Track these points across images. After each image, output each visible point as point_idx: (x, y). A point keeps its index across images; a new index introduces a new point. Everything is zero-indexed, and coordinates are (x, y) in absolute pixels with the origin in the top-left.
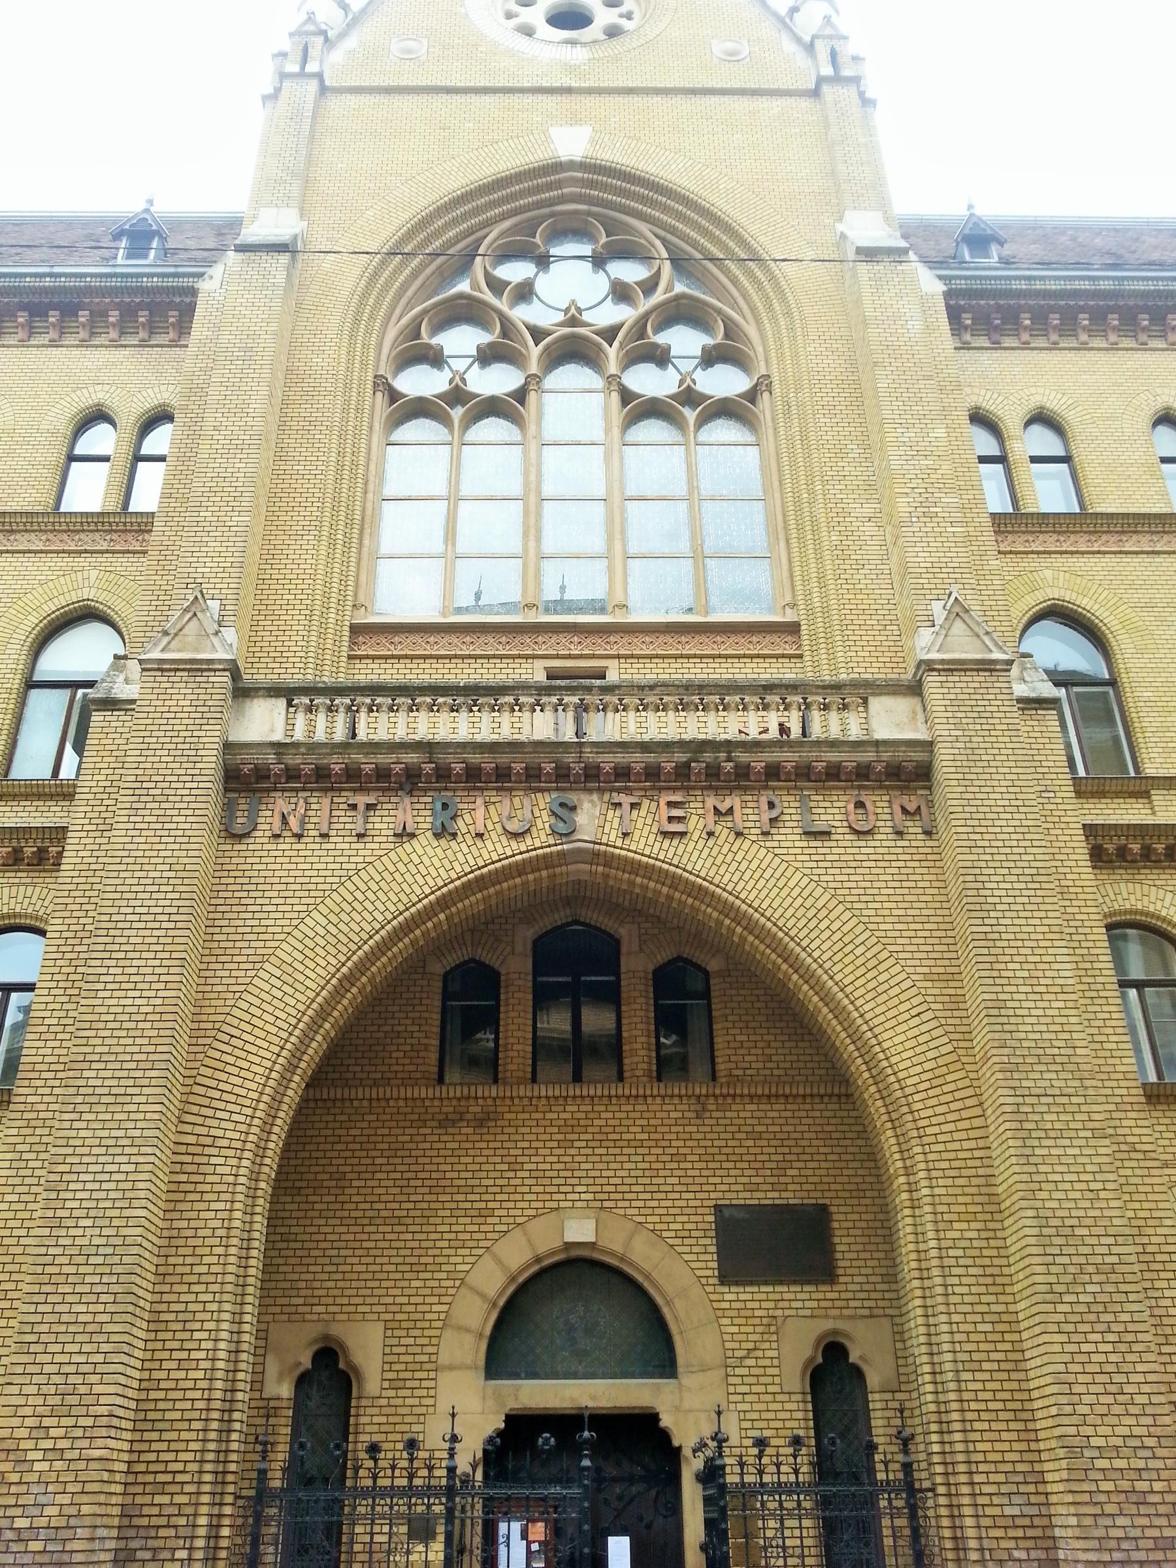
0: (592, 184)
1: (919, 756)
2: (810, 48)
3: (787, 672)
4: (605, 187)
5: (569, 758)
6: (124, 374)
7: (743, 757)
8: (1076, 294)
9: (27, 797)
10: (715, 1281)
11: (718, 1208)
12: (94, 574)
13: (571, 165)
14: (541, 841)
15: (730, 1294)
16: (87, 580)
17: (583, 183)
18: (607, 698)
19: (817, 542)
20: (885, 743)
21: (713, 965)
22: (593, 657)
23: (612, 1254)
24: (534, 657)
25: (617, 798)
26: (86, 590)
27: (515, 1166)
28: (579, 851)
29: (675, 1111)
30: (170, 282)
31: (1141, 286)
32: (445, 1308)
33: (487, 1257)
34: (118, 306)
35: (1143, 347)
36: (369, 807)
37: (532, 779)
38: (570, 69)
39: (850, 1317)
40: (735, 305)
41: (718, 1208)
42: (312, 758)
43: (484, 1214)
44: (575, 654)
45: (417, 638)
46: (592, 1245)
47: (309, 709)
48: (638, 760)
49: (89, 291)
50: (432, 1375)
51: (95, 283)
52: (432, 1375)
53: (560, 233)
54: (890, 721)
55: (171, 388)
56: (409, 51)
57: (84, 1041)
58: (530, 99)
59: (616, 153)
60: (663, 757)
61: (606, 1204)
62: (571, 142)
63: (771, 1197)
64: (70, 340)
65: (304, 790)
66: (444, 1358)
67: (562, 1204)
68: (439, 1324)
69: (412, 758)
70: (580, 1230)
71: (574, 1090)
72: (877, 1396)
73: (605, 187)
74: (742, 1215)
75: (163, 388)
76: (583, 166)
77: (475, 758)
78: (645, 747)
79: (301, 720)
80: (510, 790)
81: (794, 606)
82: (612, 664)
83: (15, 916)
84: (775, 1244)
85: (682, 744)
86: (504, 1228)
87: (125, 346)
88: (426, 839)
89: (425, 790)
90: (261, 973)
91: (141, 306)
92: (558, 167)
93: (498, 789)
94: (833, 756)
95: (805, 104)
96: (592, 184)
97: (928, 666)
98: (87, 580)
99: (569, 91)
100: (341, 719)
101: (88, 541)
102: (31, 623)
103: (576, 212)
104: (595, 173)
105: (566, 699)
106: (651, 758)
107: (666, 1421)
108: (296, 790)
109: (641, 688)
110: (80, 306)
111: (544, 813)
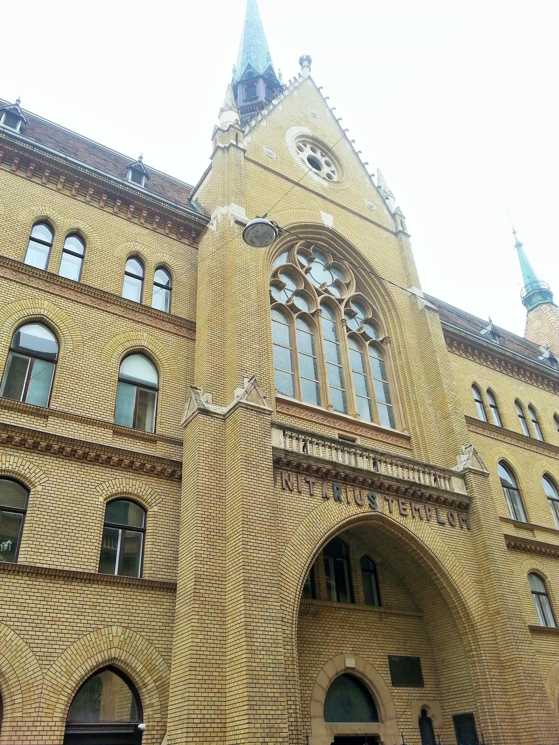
0: (332, 239)
1: (467, 501)
2: (393, 216)
3: (408, 455)
4: (336, 242)
5: (376, 479)
6: (159, 247)
7: (423, 490)
8: (455, 334)
9: (126, 435)
10: (390, 685)
11: (390, 657)
12: (145, 334)
13: (327, 229)
14: (366, 510)
15: (397, 690)
16: (145, 337)
17: (329, 237)
18: (382, 458)
19: (417, 409)
20: (458, 494)
21: (378, 560)
22: (353, 433)
23: (359, 672)
24: (335, 428)
25: (387, 497)
26: (143, 341)
27: (327, 635)
28: (377, 515)
29: (374, 617)
30: (172, 209)
31: (471, 338)
32: (310, 692)
33: (322, 672)
34: (148, 210)
35: (474, 361)
36: (314, 483)
37: (363, 484)
38: (323, 188)
39: (429, 700)
40: (375, 303)
41: (390, 657)
42: (296, 459)
43: (319, 653)
44: (349, 431)
45: (299, 410)
46: (353, 669)
47: (290, 437)
48: (395, 485)
49: (138, 198)
50: (309, 720)
51: (141, 196)
52: (309, 720)
53: (322, 253)
54: (457, 486)
55: (168, 256)
56: (270, 154)
57: (247, 571)
58: (313, 195)
59: (341, 231)
60: (304, 461)
61: (357, 652)
62: (328, 220)
63: (403, 654)
64: (135, 220)
65: (290, 471)
66: (312, 713)
67: (344, 651)
68: (309, 699)
69: (329, 467)
70: (351, 663)
71: (351, 606)
72: (437, 730)
73: (336, 242)
74: (397, 660)
75: (165, 255)
76: (331, 231)
77: (348, 472)
78: (398, 480)
79: (288, 440)
80: (355, 486)
81: (408, 429)
82: (358, 437)
83: (129, 493)
84: (406, 672)
85: (408, 482)
86: (326, 660)
87: (17, 175)
88: (332, 500)
89: (329, 480)
90: (287, 548)
91: (17, 155)
92: (323, 228)
93: (351, 485)
94: (446, 496)
95: (393, 237)
96: (332, 239)
97: (470, 470)
98: (145, 337)
99: (324, 198)
100: (302, 444)
101: (35, 283)
102: (121, 350)
103: (323, 246)
104: (334, 235)
105: (371, 455)
106: (398, 484)
107: (382, 739)
108: (287, 470)
109: (392, 456)
110: (131, 203)
111: (366, 498)
